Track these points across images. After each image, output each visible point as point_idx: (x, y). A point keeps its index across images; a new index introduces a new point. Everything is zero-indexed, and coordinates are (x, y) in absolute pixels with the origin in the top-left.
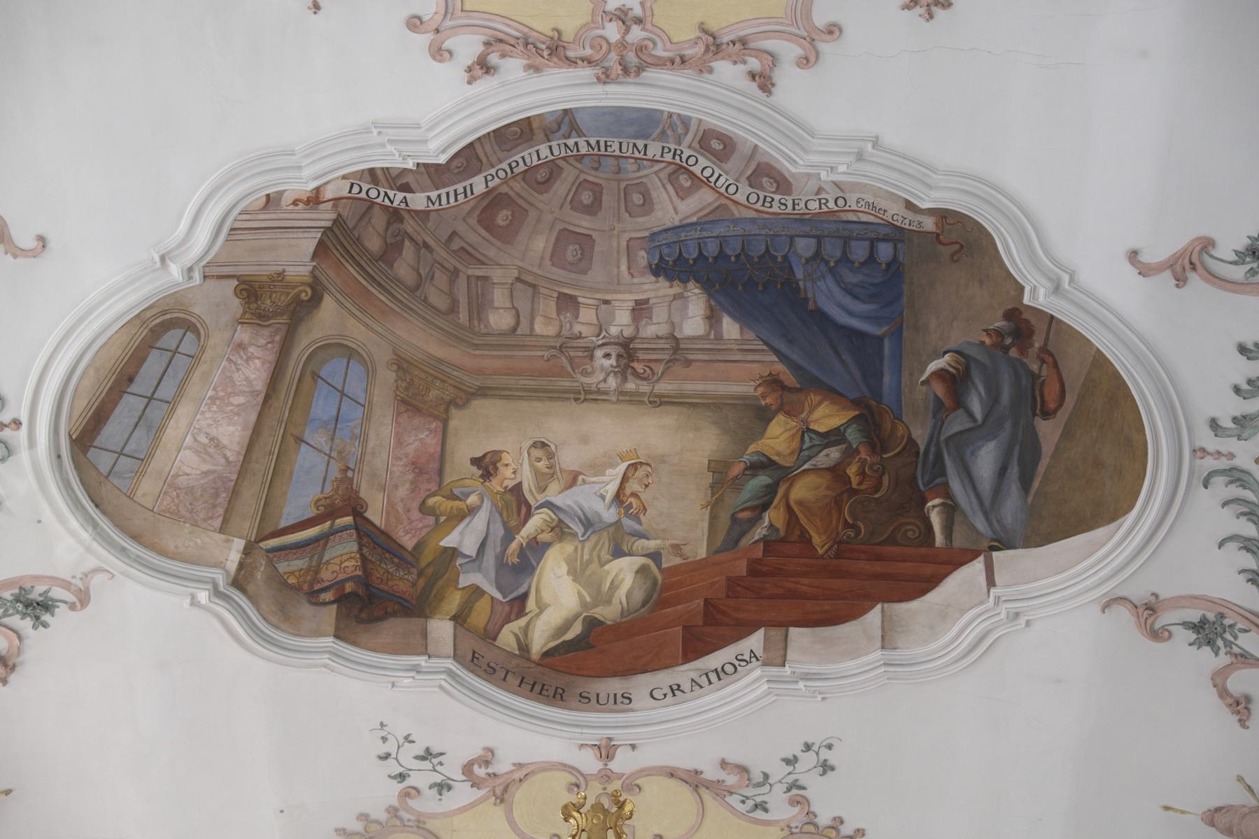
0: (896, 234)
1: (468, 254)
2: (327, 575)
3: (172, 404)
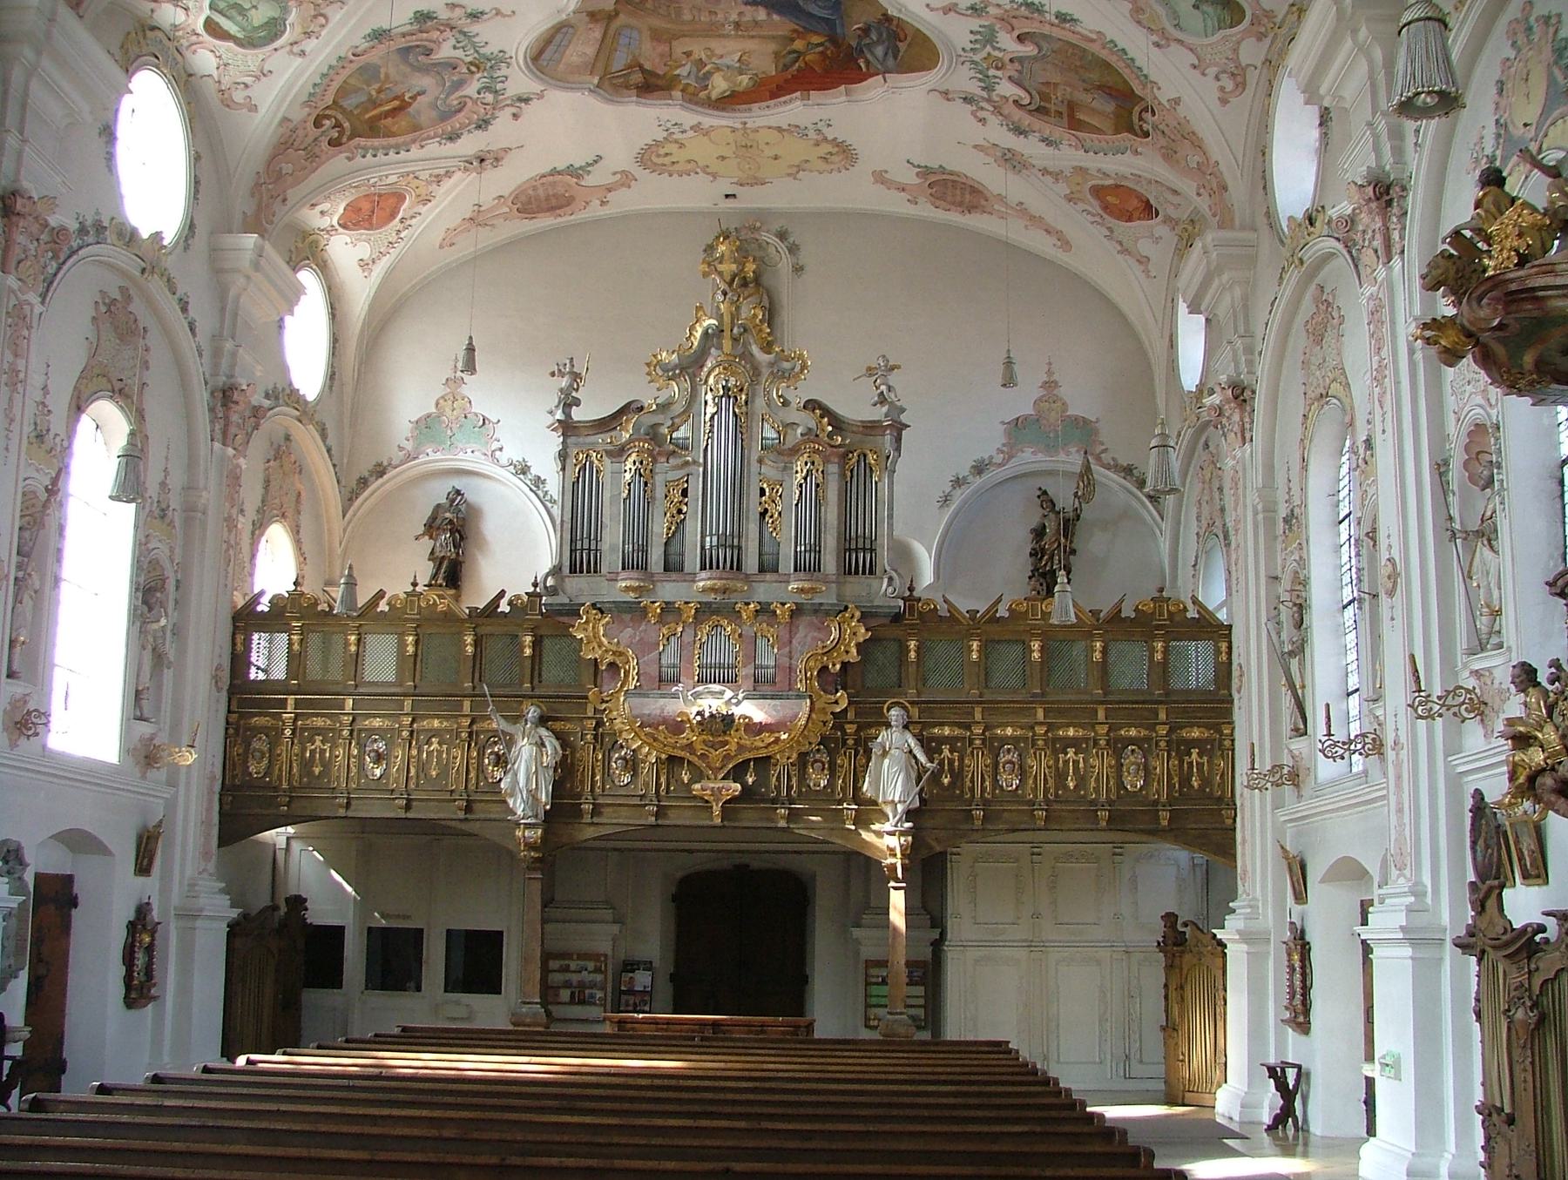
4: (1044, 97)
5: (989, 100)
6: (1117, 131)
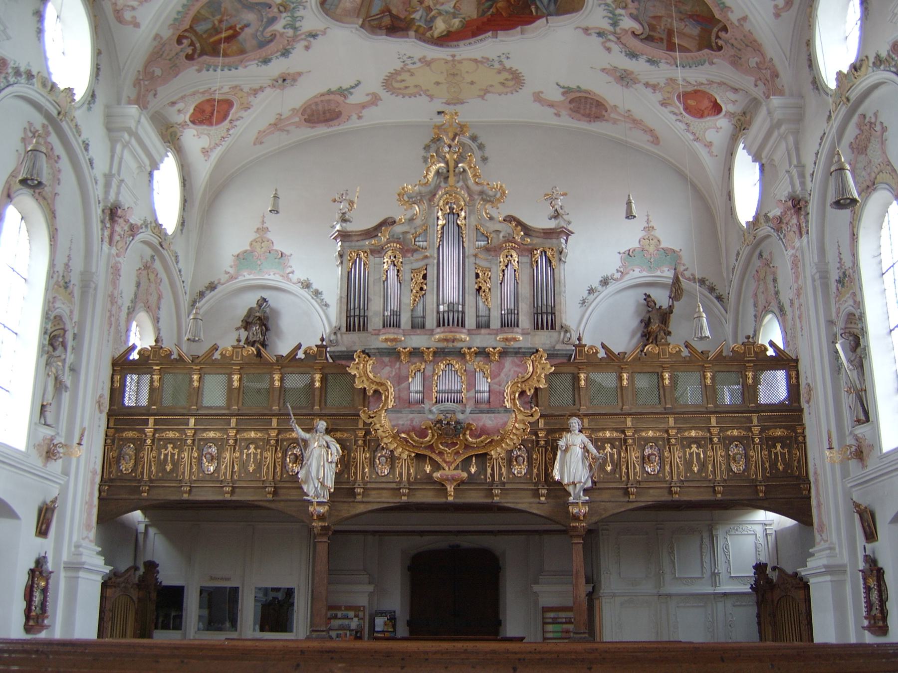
4: (652, 28)
5: (614, 33)
6: (700, 49)
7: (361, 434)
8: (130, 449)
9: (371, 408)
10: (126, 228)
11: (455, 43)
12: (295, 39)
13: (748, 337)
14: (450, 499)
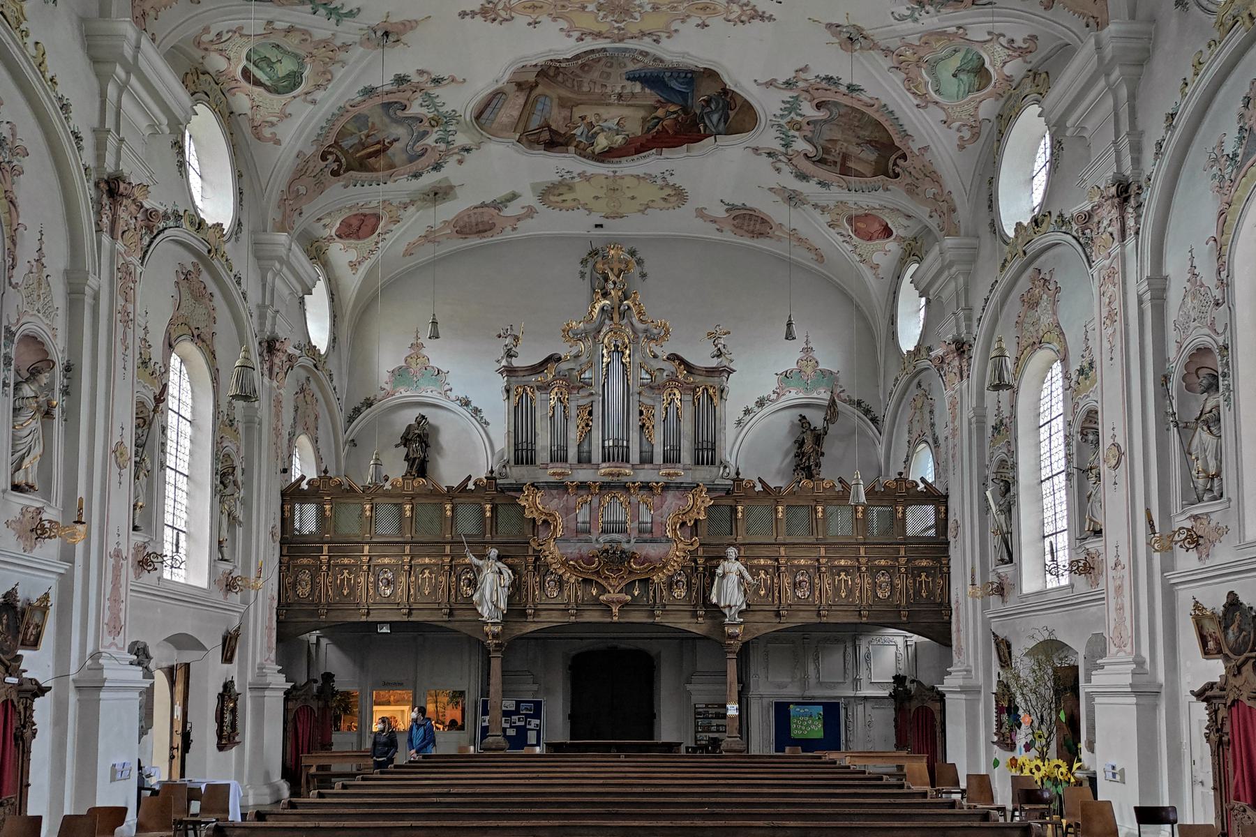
0: (692, 72)
1: (577, 76)
2: (541, 139)
3: (500, 109)
4: (826, 151)
7: (531, 559)
8: (306, 577)
9: (541, 536)
10: (284, 359)
11: (618, 159)
12: (448, 153)
13: (900, 474)
14: (615, 619)
